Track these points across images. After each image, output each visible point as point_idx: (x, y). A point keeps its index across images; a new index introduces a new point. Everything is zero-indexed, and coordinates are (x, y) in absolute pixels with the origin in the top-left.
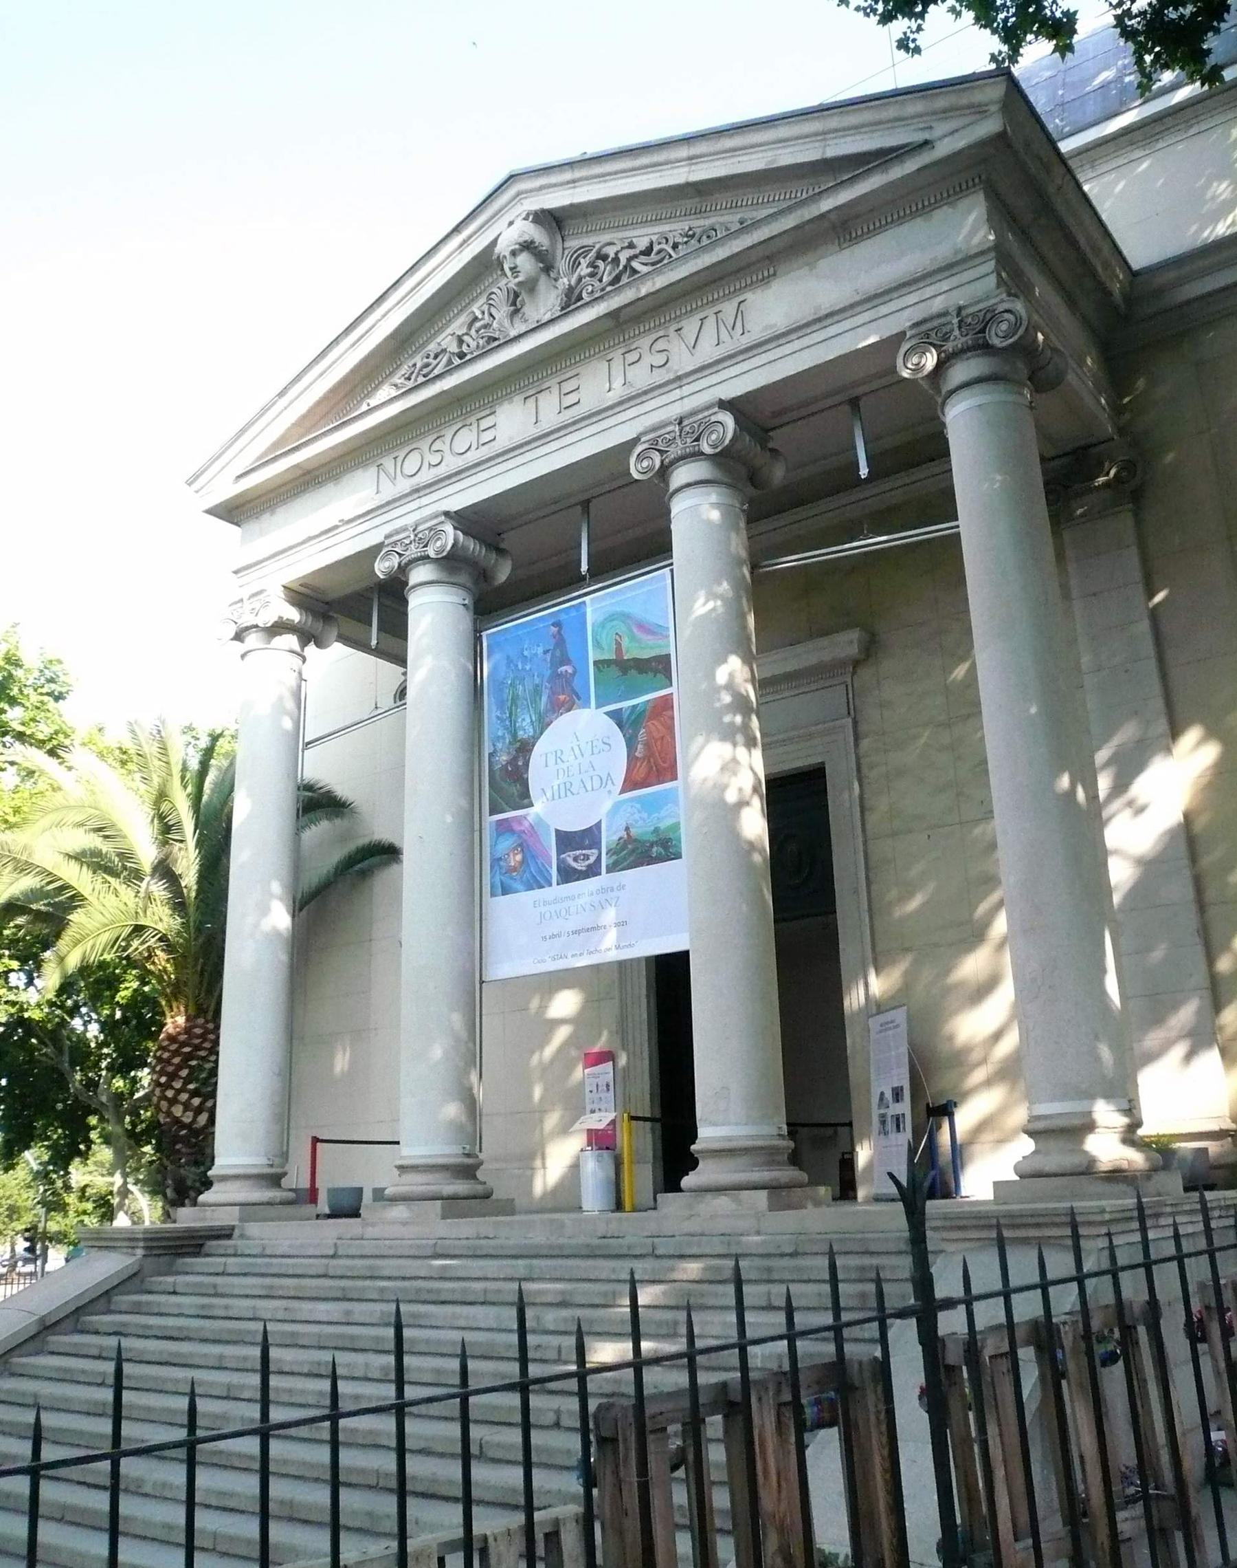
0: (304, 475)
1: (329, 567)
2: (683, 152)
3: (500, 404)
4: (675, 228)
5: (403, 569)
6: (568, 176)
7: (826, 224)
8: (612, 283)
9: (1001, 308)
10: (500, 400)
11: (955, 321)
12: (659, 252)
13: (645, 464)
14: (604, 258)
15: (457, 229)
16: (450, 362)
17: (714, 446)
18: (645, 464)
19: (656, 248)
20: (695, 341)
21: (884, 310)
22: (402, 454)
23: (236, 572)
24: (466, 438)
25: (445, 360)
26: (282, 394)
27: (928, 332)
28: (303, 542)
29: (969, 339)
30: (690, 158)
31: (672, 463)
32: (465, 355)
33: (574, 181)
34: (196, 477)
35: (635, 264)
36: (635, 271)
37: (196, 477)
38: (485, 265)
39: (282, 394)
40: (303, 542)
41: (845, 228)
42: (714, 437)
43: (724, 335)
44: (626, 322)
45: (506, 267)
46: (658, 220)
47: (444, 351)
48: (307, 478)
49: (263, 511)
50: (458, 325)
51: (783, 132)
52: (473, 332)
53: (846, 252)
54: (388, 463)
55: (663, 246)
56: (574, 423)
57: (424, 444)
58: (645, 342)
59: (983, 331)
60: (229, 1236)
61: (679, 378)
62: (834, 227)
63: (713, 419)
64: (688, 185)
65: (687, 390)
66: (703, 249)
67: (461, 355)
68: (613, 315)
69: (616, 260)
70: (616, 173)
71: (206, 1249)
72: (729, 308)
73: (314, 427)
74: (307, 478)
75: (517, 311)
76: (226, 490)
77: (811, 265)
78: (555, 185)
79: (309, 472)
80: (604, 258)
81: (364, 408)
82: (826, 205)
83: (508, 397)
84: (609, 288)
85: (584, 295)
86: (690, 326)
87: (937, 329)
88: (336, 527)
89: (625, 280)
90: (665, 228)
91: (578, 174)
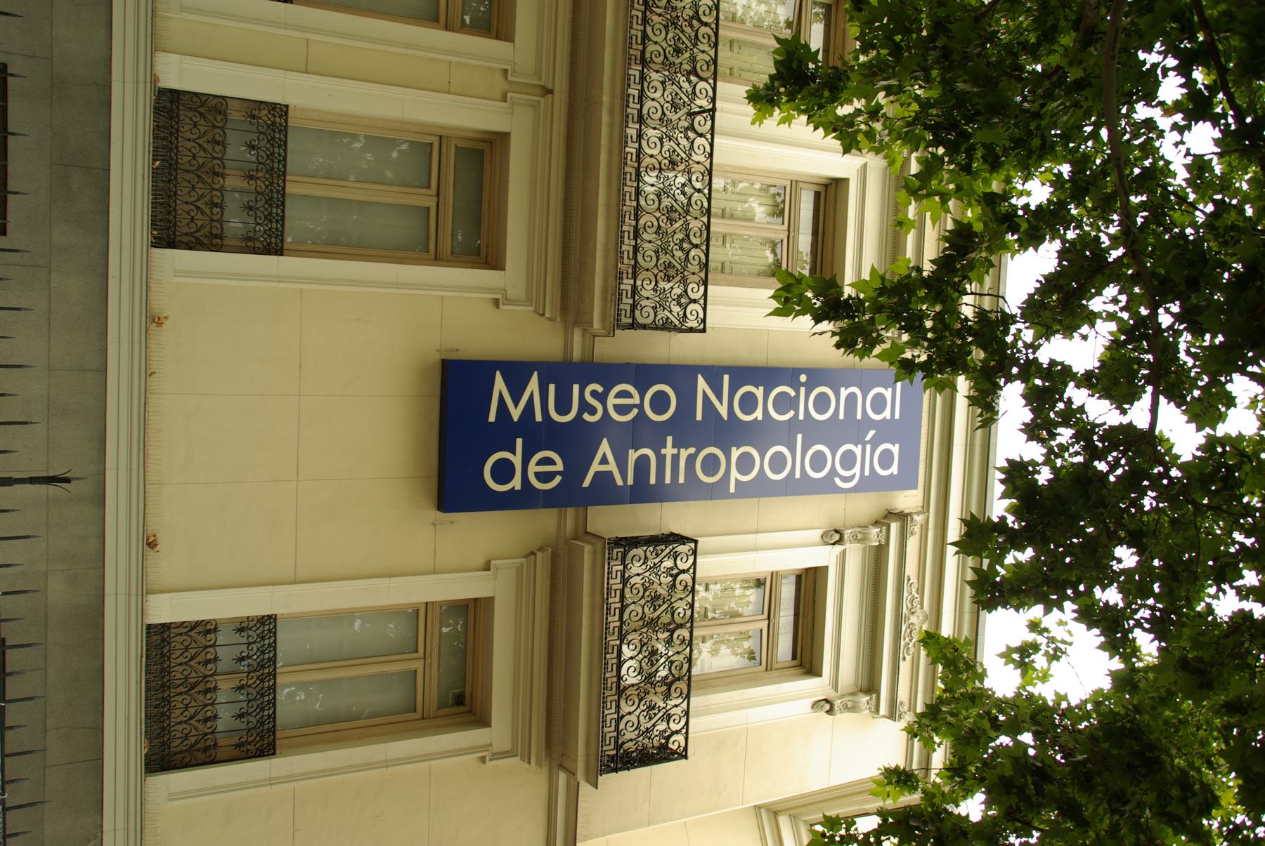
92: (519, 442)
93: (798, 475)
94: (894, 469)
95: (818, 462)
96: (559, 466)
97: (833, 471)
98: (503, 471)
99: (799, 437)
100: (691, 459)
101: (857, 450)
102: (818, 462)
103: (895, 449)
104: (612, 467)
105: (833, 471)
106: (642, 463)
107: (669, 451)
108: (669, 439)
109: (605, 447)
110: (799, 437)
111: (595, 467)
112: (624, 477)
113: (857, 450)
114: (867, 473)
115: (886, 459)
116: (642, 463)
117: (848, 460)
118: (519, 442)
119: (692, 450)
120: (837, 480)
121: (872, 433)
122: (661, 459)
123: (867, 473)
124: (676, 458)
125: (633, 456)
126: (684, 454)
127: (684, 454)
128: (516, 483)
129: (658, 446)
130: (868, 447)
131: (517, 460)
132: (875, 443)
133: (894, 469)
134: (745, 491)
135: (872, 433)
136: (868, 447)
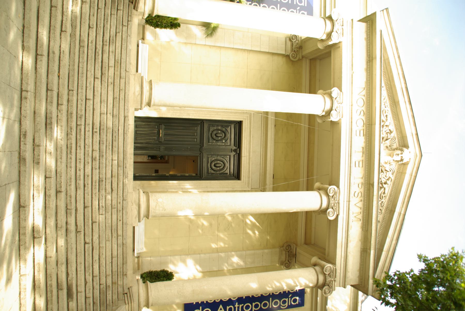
0: (372, 57)
1: (341, 63)
2: (403, 212)
3: (365, 138)
4: (385, 201)
5: (331, 98)
6: (414, 174)
7: (368, 248)
8: (381, 181)
9: (331, 290)
10: (366, 139)
11: (333, 279)
12: (383, 197)
13: (332, 191)
14: (388, 179)
15: (417, 134)
16: (383, 121)
17: (328, 213)
18: (332, 191)
19: (384, 196)
20: (356, 207)
21: (343, 259)
22: (364, 98)
23: (352, 20)
24: (361, 124)
25: (385, 120)
26: (399, 57)
27: (333, 273)
28: (352, 54)
29: (328, 282)
30: (400, 213)
31: (329, 199)
32: (383, 127)
33: (411, 175)
34: (388, 13)
35: (383, 189)
36: (381, 188)
37: (388, 13)
38: (404, 145)
39: (399, 57)
40: (352, 54)
41: (365, 251)
42: (331, 213)
43: (355, 215)
44: (370, 187)
45: (399, 152)
46: (391, 195)
47: (387, 120)
48: (371, 58)
49: (367, 35)
50: (392, 127)
51: (394, 242)
52: (388, 131)
53: (359, 249)
54: (364, 93)
55: (384, 198)
56: (350, 167)
57: (364, 108)
58: (362, 190)
59: (328, 285)
60: (134, 8)
61: (349, 201)
62: (367, 249)
63: (335, 213)
64: (394, 211)
65: (345, 202)
66: (377, 211)
68: (373, 185)
70: (407, 190)
71: (130, 3)
72: (360, 216)
73: (384, 60)
74: (371, 58)
75: (387, 147)
76: (380, 24)
77: (361, 240)
78: (413, 169)
79: (372, 60)
81: (383, 84)
82: (372, 252)
83: (366, 142)
84: (380, 180)
85: (382, 173)
86: (360, 205)
87: (333, 275)
88: (352, 70)
89: (380, 185)
90: (387, 197)
91: (413, 177)
92: (201, 307)
93: (270, 307)
97: (280, 305)
99: (271, 299)
100: (242, 307)
101: (287, 300)
105: (280, 305)
107: (237, 305)
108: (237, 303)
109: (221, 306)
110: (271, 299)
113: (287, 300)
114: (289, 304)
117: (284, 302)
118: (201, 307)
119: (243, 305)
120: (281, 307)
121: (291, 295)
122: (235, 308)
123: (289, 304)
124: (238, 307)
125: (228, 308)
126: (241, 306)
127: (241, 306)
130: (290, 299)
132: (291, 297)
133: (297, 303)
135: (291, 295)
136: (290, 299)
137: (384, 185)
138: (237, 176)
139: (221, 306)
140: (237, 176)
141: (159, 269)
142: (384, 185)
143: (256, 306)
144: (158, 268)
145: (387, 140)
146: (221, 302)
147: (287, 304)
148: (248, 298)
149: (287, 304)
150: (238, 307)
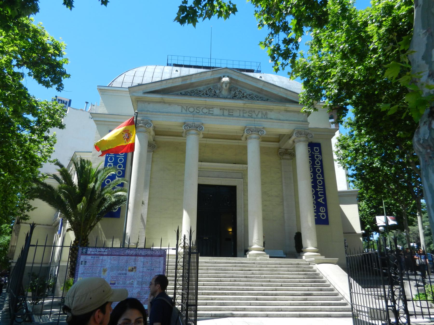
35: (247, 96)
67: (207, 94)
69: (243, 94)
80: (241, 92)
94: (318, 148)
95: (318, 163)
96: (322, 207)
97: (319, 160)
98: (323, 216)
100: (320, 186)
101: (316, 155)
102: (318, 163)
103: (315, 148)
104: (321, 199)
105: (319, 160)
106: (321, 194)
107: (318, 190)
109: (319, 200)
111: (321, 202)
112: (322, 197)
113: (316, 155)
115: (317, 150)
116: (321, 194)
117: (317, 157)
122: (320, 191)
124: (320, 188)
125: (320, 196)
126: (319, 187)
127: (319, 187)
128: (324, 214)
129: (318, 191)
131: (321, 214)
132: (314, 152)
134: (323, 177)
137: (245, 95)
138: (233, 189)
139: (319, 200)
140: (233, 189)
141: (294, 241)
142: (245, 95)
143: (319, 176)
144: (293, 241)
145: (215, 92)
146: (316, 200)
147: (318, 155)
148: (313, 187)
149: (318, 155)
150: (320, 188)
